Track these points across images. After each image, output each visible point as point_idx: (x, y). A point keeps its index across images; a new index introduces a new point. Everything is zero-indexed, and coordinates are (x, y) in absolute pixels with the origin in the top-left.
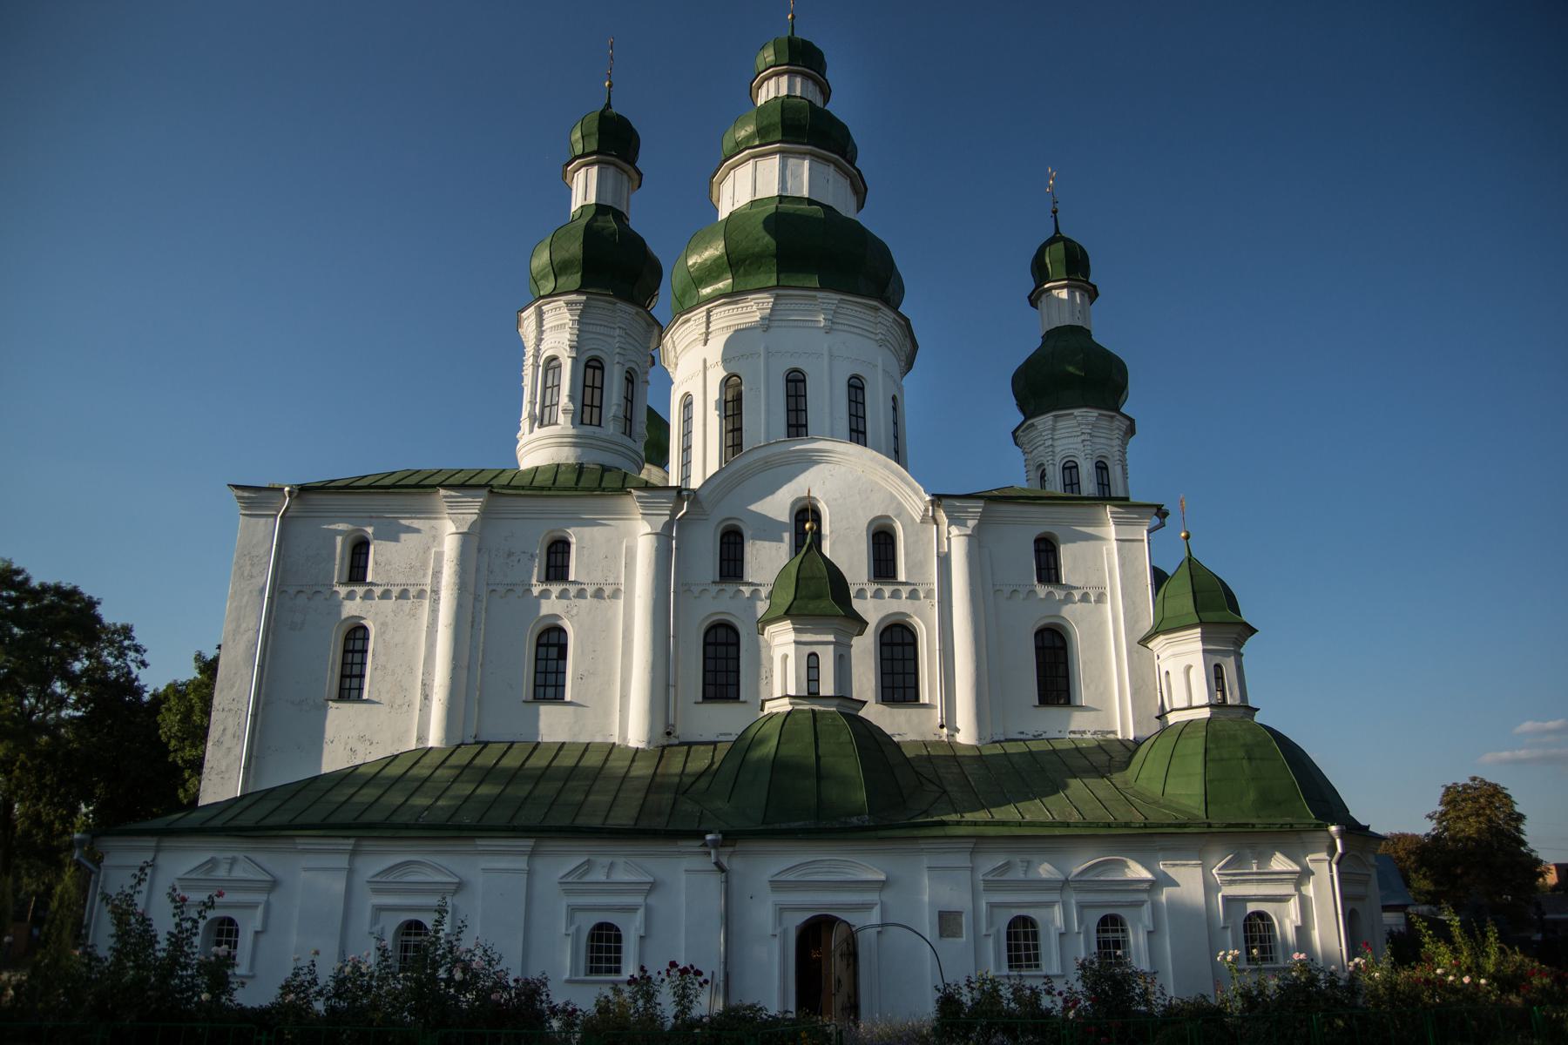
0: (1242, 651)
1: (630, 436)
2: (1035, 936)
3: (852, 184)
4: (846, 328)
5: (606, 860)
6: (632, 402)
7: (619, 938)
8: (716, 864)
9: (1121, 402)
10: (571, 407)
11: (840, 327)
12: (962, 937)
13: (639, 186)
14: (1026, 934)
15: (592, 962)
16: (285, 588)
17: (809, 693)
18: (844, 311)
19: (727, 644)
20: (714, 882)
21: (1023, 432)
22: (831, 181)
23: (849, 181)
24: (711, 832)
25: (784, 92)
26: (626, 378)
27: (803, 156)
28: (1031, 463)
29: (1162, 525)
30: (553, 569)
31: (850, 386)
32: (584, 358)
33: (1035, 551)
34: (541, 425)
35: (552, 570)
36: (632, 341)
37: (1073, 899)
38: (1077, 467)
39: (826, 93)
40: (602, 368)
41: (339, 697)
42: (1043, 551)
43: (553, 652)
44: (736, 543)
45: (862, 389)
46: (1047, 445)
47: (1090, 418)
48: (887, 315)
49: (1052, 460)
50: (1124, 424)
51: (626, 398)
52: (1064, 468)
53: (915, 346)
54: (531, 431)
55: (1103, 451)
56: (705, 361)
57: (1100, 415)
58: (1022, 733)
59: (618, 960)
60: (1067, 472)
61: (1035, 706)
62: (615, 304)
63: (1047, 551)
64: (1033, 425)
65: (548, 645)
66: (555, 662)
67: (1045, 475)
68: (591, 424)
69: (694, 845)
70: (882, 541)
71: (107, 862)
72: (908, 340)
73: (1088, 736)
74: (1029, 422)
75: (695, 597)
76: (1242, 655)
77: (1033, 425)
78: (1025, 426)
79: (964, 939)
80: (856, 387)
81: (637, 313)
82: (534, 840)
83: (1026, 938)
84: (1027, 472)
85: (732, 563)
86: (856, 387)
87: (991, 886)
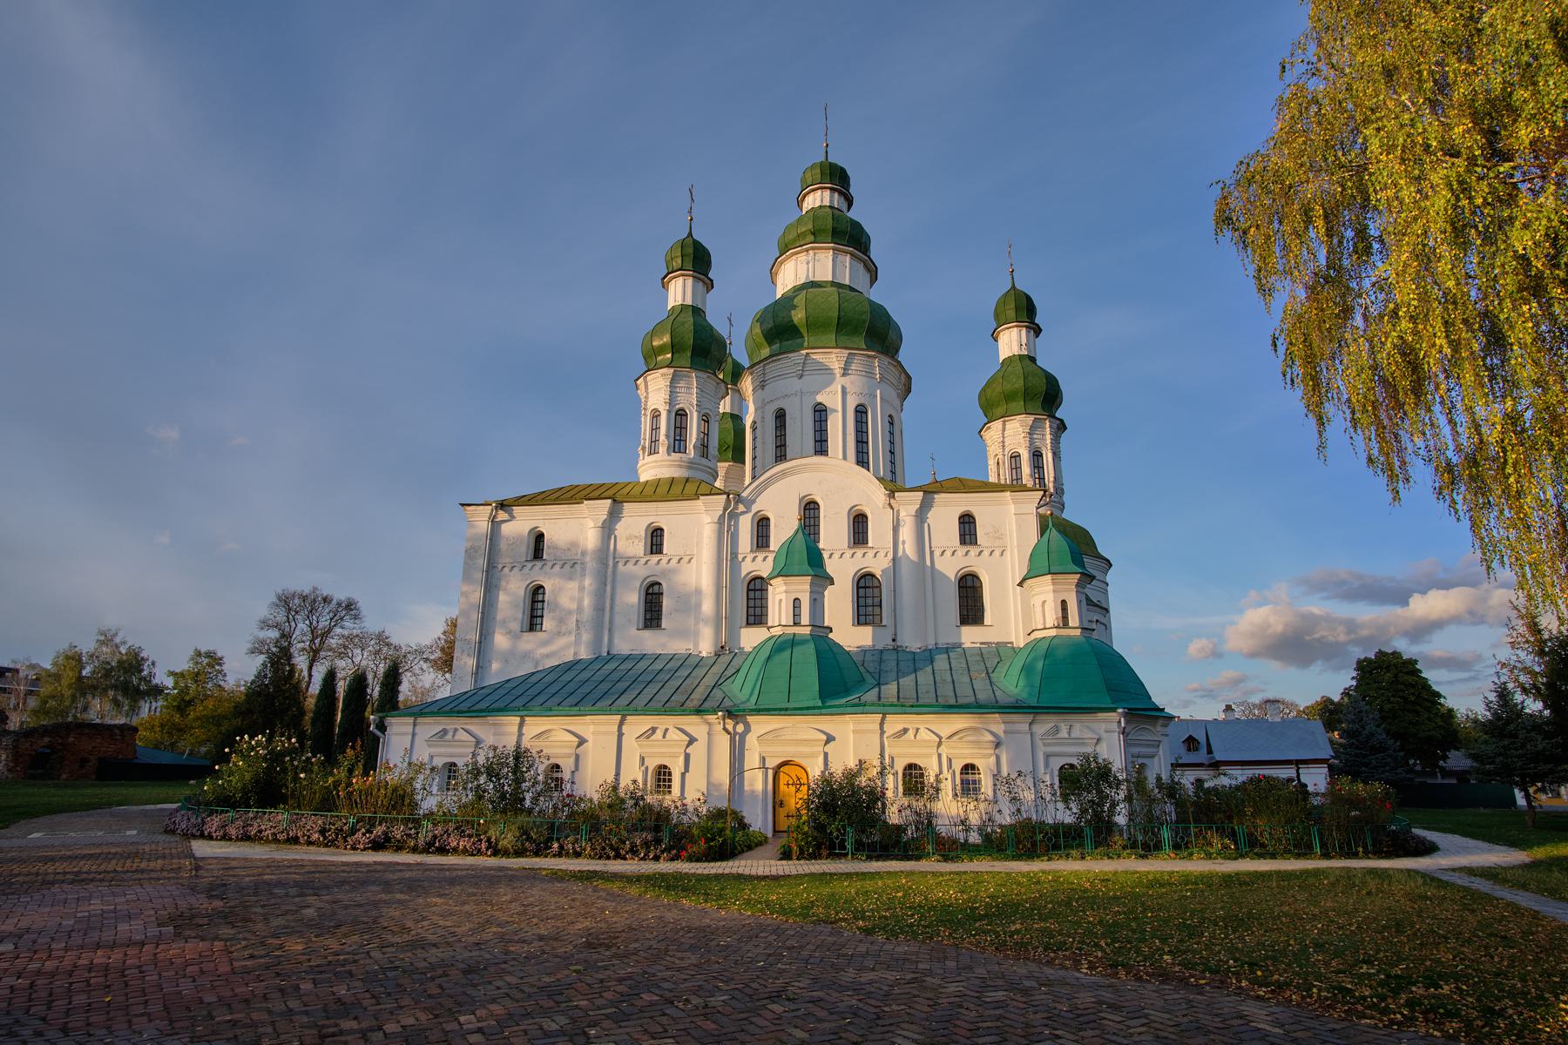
3: (866, 266)
7: (670, 774)
34: (650, 454)
39: (850, 202)
48: (886, 360)
53: (909, 378)
60: (1013, 460)
63: (969, 523)
86: (861, 412)
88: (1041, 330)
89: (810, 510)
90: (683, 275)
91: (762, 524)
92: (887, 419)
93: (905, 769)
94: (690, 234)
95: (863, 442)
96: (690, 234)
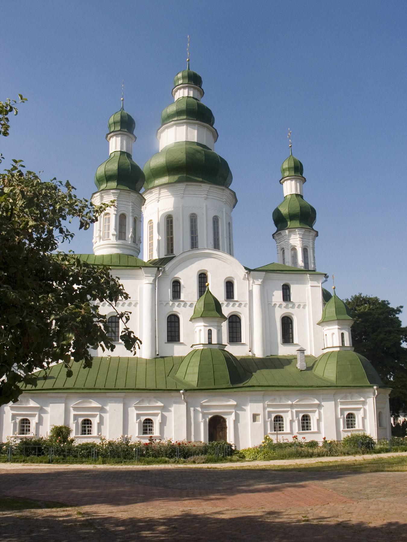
4: (212, 197)
7: (152, 423)
9: (313, 224)
10: (115, 233)
11: (210, 197)
12: (259, 421)
13: (135, 141)
15: (144, 431)
18: (211, 191)
19: (175, 322)
24: (182, 390)
25: (186, 95)
28: (279, 247)
29: (326, 281)
32: (119, 214)
37: (294, 410)
44: (177, 286)
50: (313, 234)
54: (100, 241)
56: (158, 209)
64: (280, 233)
70: (229, 285)
72: (234, 199)
74: (279, 232)
75: (165, 306)
78: (277, 233)
79: (260, 422)
86: (216, 220)
87: (269, 406)
88: (305, 180)
89: (203, 277)
90: (120, 134)
91: (176, 285)
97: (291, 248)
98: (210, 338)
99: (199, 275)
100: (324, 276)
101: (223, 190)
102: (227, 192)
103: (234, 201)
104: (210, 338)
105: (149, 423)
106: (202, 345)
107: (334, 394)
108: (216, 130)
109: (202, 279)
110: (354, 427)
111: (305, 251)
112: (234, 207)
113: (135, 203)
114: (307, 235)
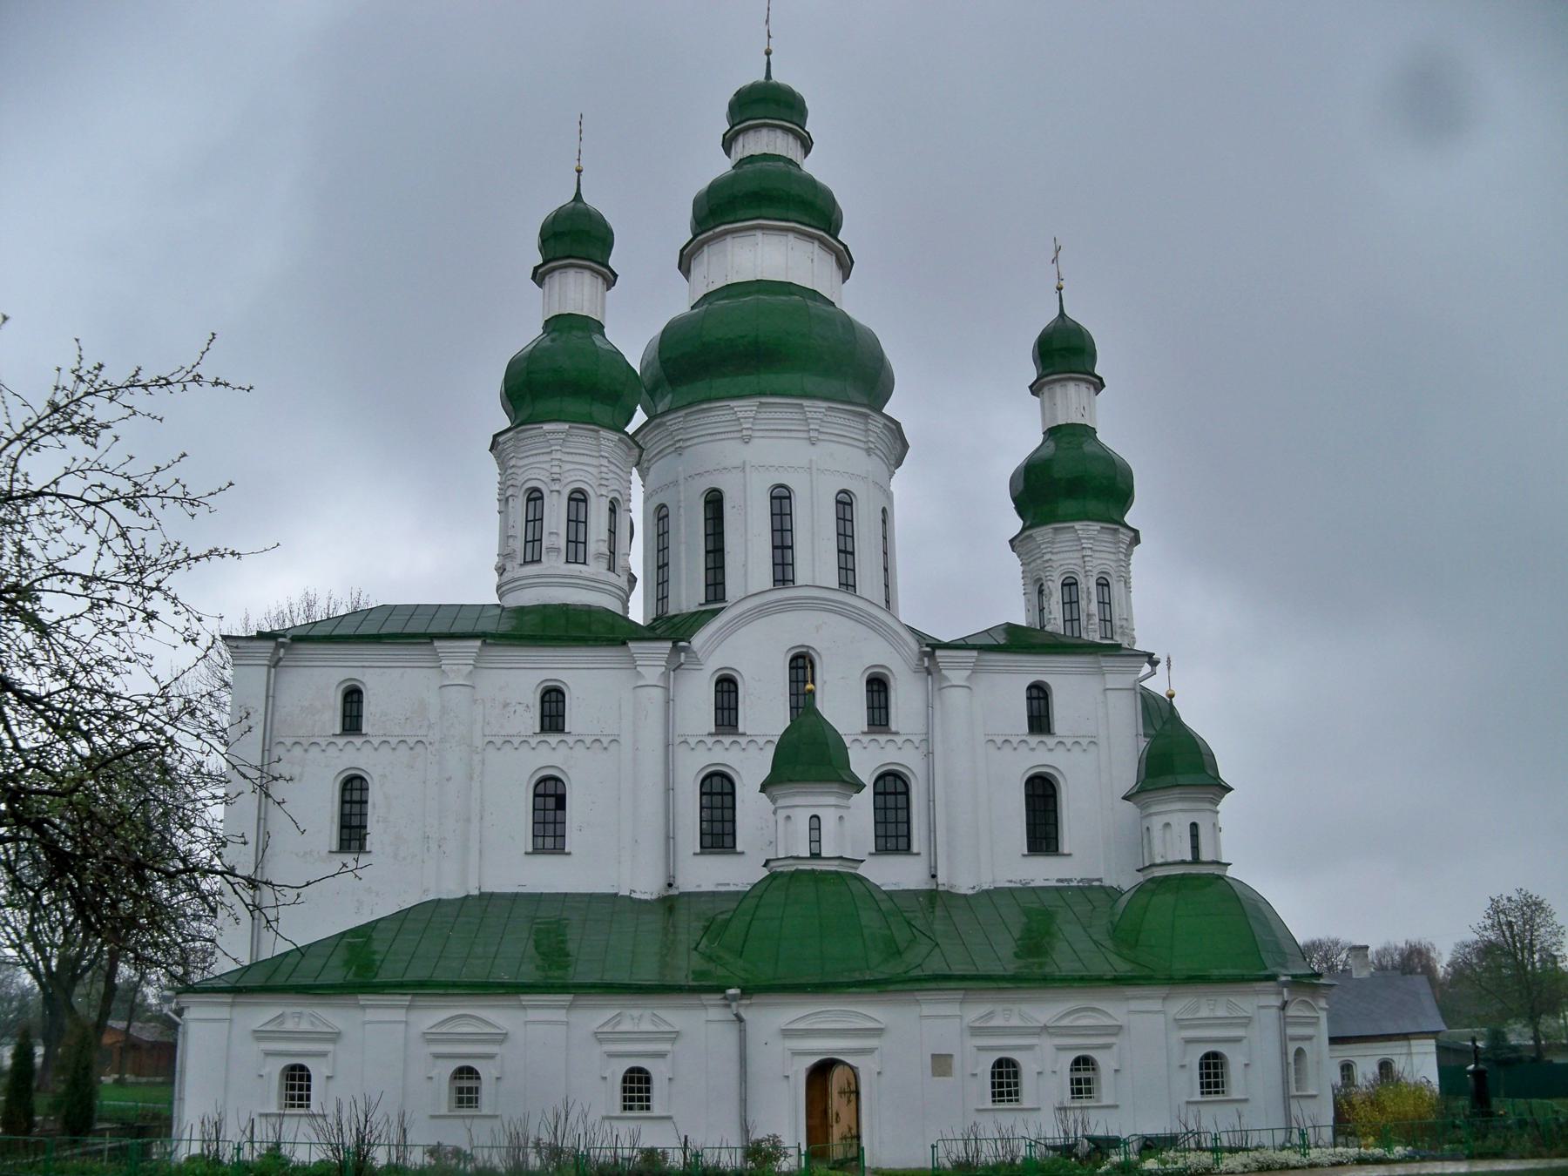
0: (1219, 808)
1: (614, 572)
2: (1016, 1075)
5: (636, 1013)
6: (614, 533)
7: (648, 1080)
8: (737, 1015)
14: (1008, 1073)
16: (282, 740)
17: (811, 854)
20: (734, 1028)
21: (1020, 541)
22: (815, 260)
23: (834, 258)
26: (610, 509)
27: (785, 233)
28: (1029, 575)
30: (548, 718)
31: (838, 502)
33: (1028, 698)
34: (525, 563)
35: (547, 720)
36: (613, 468)
38: (1076, 584)
39: (806, 145)
40: (585, 501)
41: (341, 848)
42: (1034, 698)
43: (551, 802)
44: (729, 692)
45: (851, 504)
46: (1045, 559)
47: (1091, 532)
49: (1050, 576)
50: (1125, 537)
51: (610, 530)
52: (1063, 585)
53: (905, 446)
55: (1102, 566)
57: (1102, 528)
58: (1011, 881)
59: (648, 1099)
60: (1066, 588)
61: (1024, 855)
62: (597, 431)
63: (1039, 698)
65: (545, 795)
66: (553, 812)
67: (1043, 590)
68: (576, 562)
69: (715, 998)
71: (186, 1015)
72: (899, 442)
73: (1074, 884)
74: (1027, 533)
76: (1218, 812)
77: (1030, 536)
80: (845, 503)
81: (620, 440)
82: (572, 995)
83: (1008, 1077)
84: (1024, 585)
85: (726, 705)
86: (845, 503)
87: (976, 1031)
88: (1103, 386)
89: (802, 665)
91: (727, 687)
92: (880, 516)
93: (993, 1067)
94: (578, 197)
95: (845, 552)
96: (578, 197)
97: (1064, 577)
98: (815, 840)
99: (791, 661)
100: (1147, 659)
101: (866, 416)
102: (876, 424)
103: (898, 446)
104: (815, 840)
105: (640, 1081)
106: (791, 862)
107: (1164, 999)
108: (845, 246)
109: (801, 672)
110: (1223, 1092)
111: (1103, 584)
112: (899, 463)
113: (612, 460)
114: (1106, 542)
